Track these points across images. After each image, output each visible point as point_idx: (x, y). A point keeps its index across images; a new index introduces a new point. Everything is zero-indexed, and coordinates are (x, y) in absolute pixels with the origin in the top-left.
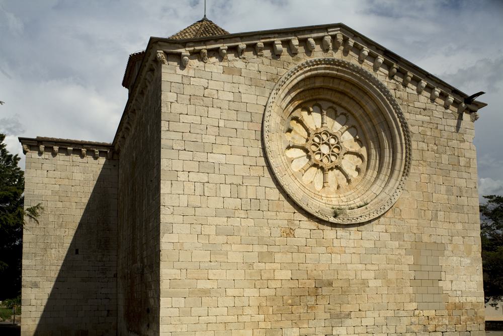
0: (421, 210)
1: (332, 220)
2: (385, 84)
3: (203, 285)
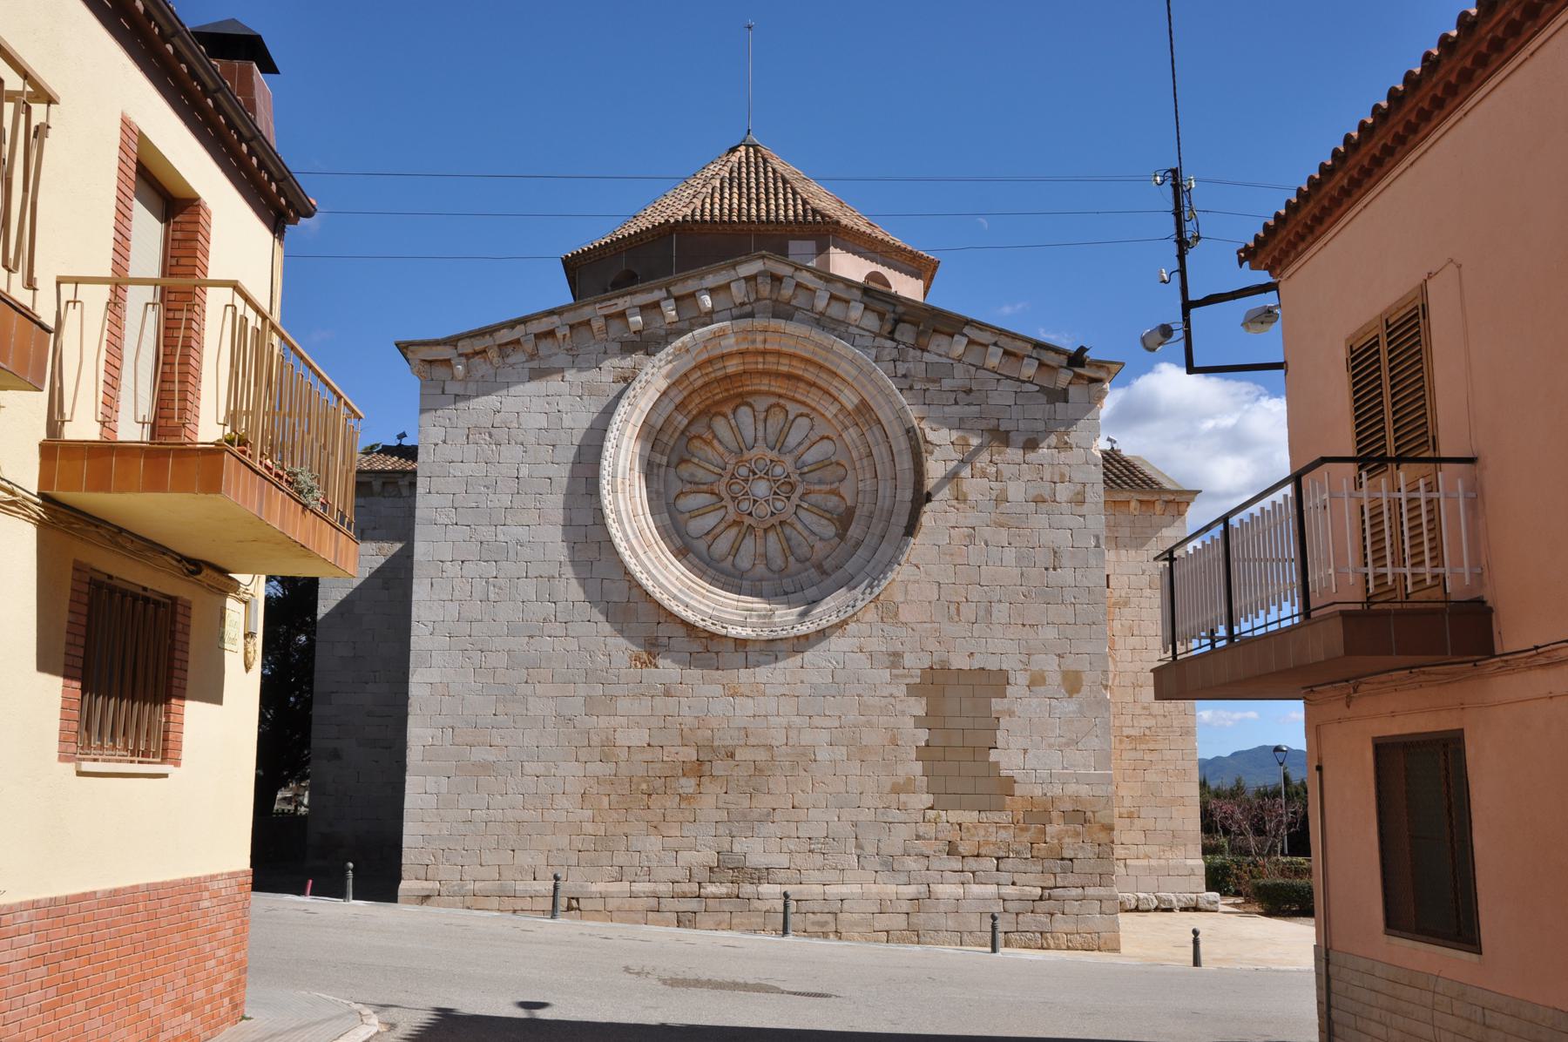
3: (480, 754)
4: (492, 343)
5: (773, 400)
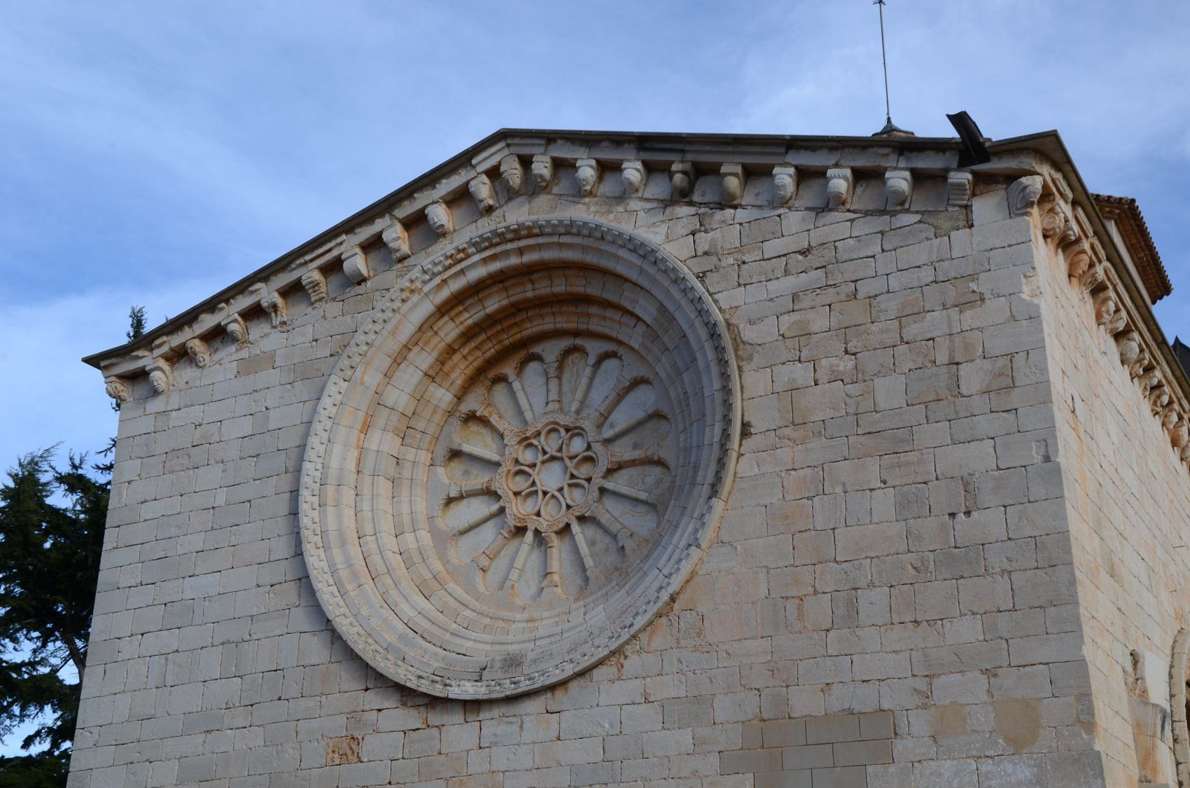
5: (566, 343)
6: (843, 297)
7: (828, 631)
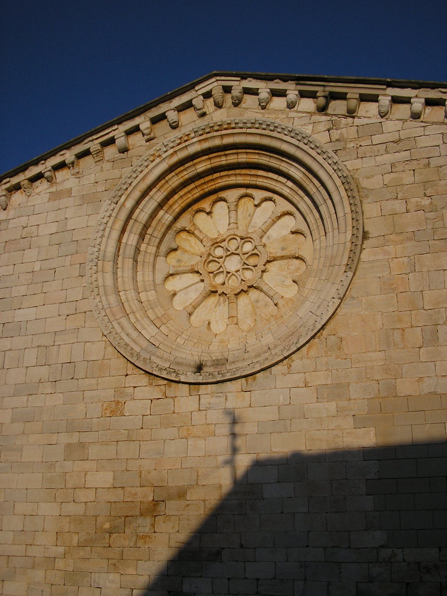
0: (394, 329)
1: (192, 378)
2: (308, 130)
4: (24, 178)
6: (422, 166)
7: (420, 348)
